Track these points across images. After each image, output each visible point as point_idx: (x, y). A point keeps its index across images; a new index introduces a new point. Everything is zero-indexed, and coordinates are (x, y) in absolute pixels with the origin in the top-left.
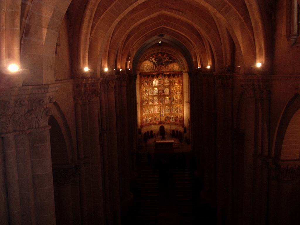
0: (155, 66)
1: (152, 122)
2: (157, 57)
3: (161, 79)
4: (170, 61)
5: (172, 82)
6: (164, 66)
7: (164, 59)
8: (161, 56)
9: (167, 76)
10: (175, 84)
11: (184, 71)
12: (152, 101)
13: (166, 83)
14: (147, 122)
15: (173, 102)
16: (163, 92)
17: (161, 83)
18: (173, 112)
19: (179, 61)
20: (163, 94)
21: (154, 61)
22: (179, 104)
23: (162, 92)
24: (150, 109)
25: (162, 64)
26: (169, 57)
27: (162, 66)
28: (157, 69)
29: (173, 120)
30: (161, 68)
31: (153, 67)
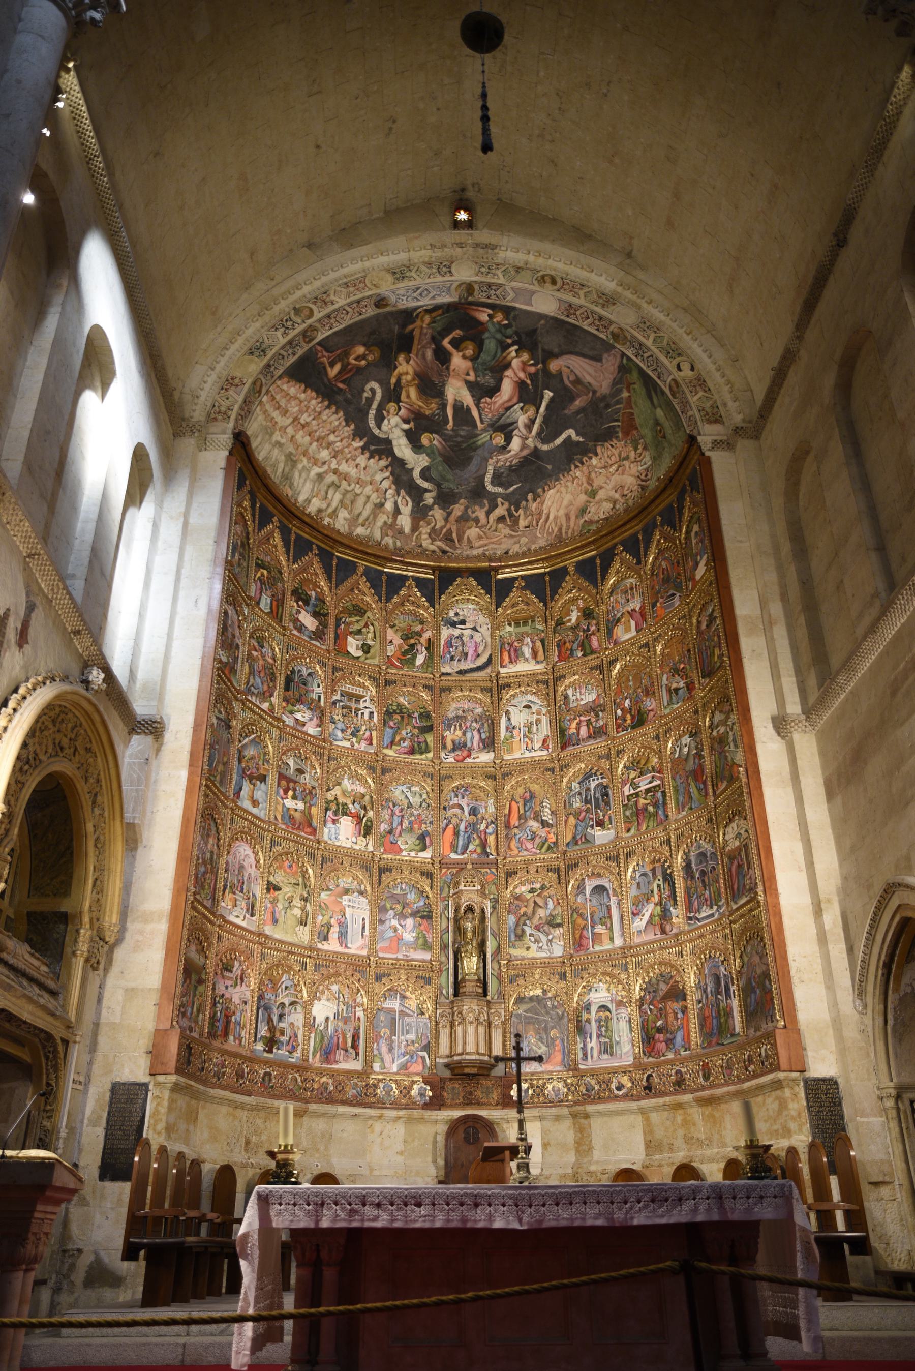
0: (406, 509)
1: (356, 1065)
2: (430, 408)
3: (463, 622)
4: (559, 441)
5: (574, 628)
6: (500, 511)
7: (499, 440)
8: (468, 399)
9: (523, 588)
10: (610, 632)
11: (707, 435)
12: (358, 819)
13: (516, 656)
14: (271, 1043)
15: (601, 824)
16: (489, 743)
17: (466, 655)
18: (607, 946)
19: (662, 358)
20: (486, 757)
21: (402, 448)
22: (684, 813)
23: (473, 739)
24: (324, 895)
25: (478, 493)
26: (548, 394)
27: (481, 514)
28: (434, 534)
29: (607, 1049)
30: (472, 532)
31: (389, 506)
